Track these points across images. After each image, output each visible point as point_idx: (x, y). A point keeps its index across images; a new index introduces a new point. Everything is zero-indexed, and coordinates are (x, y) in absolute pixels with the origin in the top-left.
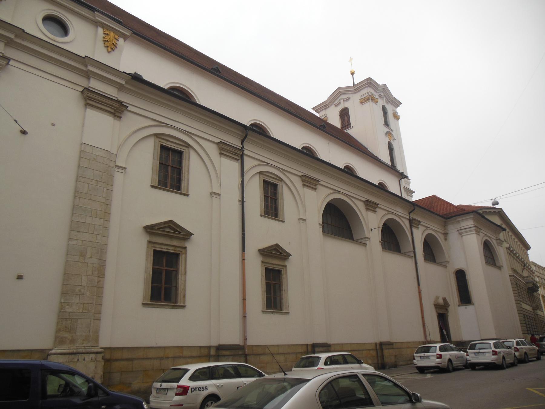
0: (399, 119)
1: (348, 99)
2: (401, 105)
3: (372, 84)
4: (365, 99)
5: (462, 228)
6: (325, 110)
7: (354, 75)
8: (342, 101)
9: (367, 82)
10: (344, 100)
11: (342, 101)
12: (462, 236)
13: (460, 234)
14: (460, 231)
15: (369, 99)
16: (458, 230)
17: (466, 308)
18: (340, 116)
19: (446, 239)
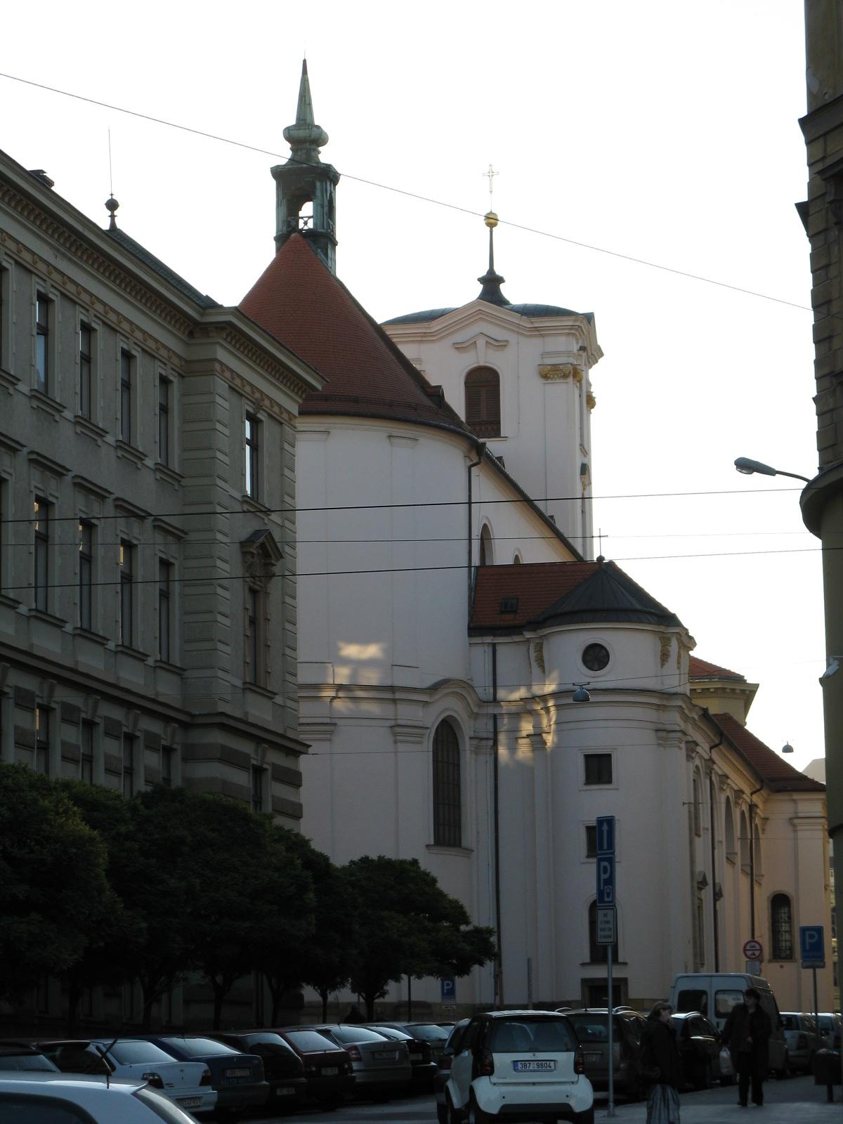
0: (593, 407)
1: (502, 345)
2: (601, 360)
3: (582, 330)
4: (555, 368)
5: (800, 815)
6: (417, 344)
7: (494, 229)
8: (481, 342)
9: (571, 324)
10: (487, 342)
11: (481, 342)
12: (795, 831)
13: (794, 826)
14: (796, 821)
15: (565, 376)
16: (791, 819)
17: (782, 967)
18: (465, 383)
19: (763, 830)
